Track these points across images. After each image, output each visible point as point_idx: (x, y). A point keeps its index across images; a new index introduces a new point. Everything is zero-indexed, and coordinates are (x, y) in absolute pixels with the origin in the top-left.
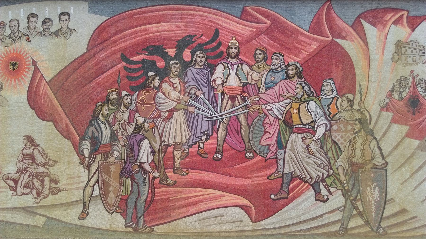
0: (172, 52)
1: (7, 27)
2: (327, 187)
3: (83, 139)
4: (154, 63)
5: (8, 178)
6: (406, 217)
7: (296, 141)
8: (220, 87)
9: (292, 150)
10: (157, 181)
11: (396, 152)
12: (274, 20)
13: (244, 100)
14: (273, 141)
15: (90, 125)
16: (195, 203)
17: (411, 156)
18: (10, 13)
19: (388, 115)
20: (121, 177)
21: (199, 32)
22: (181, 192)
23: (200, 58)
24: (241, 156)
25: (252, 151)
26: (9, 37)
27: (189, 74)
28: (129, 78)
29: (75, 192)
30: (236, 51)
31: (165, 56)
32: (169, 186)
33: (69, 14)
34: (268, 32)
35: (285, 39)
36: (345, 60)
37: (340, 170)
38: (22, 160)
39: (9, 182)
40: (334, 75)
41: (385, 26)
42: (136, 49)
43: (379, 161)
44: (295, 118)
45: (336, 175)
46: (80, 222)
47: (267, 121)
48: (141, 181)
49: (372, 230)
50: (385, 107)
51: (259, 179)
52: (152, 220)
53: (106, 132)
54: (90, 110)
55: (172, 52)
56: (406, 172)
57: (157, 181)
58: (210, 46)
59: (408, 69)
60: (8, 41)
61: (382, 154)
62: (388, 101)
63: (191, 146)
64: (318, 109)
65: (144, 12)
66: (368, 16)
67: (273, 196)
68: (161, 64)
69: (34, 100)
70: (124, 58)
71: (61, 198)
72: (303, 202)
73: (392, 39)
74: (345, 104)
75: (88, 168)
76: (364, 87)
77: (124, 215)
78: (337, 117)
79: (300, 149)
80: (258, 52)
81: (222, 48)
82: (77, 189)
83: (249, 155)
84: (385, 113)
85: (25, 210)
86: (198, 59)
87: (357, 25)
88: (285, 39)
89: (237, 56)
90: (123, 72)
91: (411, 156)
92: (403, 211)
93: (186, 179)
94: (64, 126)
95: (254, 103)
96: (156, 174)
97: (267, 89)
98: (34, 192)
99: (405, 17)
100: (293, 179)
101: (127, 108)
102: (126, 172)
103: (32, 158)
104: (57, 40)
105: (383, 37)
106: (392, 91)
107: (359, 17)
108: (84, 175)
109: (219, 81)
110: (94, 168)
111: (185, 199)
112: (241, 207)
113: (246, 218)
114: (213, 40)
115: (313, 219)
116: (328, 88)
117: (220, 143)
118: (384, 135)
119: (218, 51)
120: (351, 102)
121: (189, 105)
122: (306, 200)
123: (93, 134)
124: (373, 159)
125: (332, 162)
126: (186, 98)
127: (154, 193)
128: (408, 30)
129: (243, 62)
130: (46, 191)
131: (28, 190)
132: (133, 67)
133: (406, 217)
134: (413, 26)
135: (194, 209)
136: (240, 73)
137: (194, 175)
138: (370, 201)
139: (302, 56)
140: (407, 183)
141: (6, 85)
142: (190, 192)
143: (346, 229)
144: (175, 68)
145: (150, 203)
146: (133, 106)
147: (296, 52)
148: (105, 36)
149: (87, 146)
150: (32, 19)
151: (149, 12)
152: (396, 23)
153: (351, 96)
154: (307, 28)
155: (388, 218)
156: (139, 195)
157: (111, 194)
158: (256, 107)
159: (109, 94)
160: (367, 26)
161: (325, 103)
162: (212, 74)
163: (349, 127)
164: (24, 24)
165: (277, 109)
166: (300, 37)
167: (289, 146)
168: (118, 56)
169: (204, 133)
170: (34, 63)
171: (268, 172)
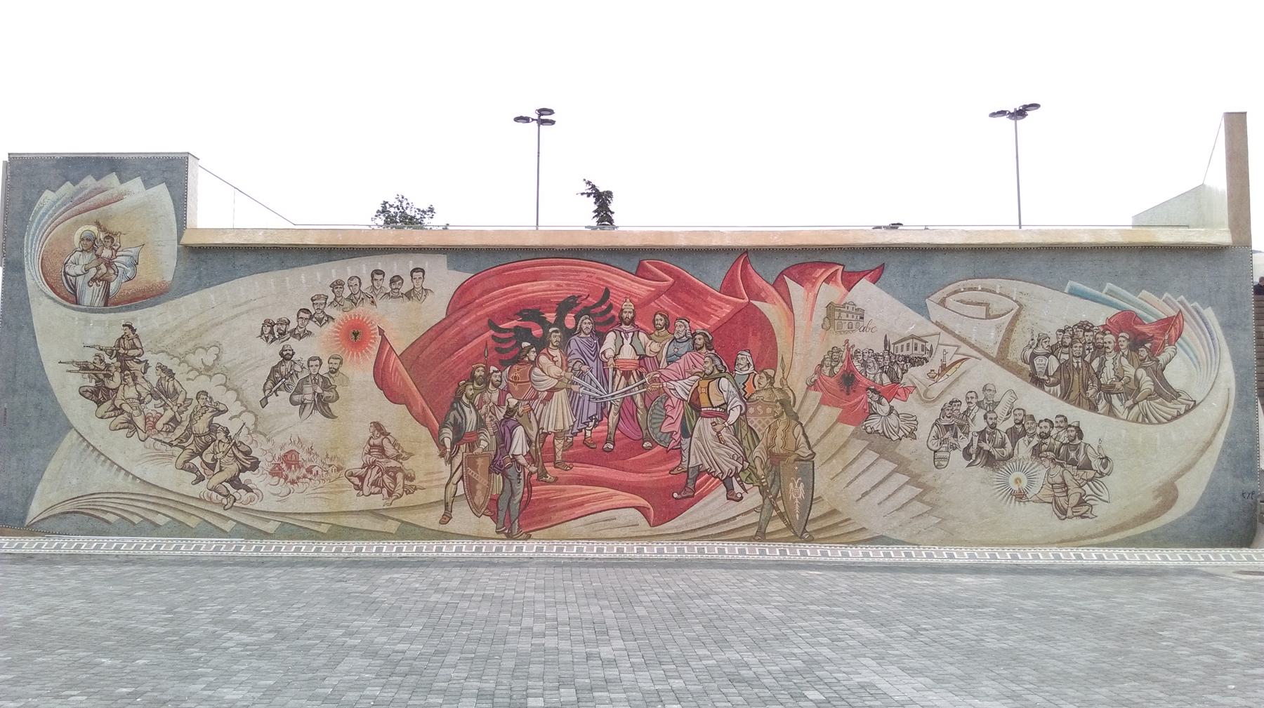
0: (551, 317)
1: (346, 286)
2: (741, 483)
3: (443, 426)
4: (530, 330)
5: (352, 475)
6: (837, 519)
7: (704, 427)
8: (611, 361)
9: (699, 438)
10: (535, 477)
11: (825, 441)
12: (677, 277)
13: (641, 377)
14: (677, 427)
15: (452, 408)
16: (582, 504)
17: (844, 446)
18: (349, 269)
19: (816, 395)
20: (490, 472)
21: (584, 292)
22: (564, 490)
23: (586, 324)
24: (637, 446)
25: (651, 440)
26: (349, 299)
27: (573, 344)
28: (498, 350)
29: (435, 491)
30: (631, 315)
31: (543, 322)
32: (549, 483)
33: (423, 271)
34: (670, 291)
35: (691, 301)
36: (764, 327)
37: (757, 462)
38: (369, 453)
39: (353, 479)
40: (750, 347)
41: (814, 284)
42: (506, 314)
44: (703, 398)
45: (752, 468)
46: (442, 528)
47: (669, 402)
48: (514, 477)
49: (796, 535)
50: (813, 385)
51: (659, 475)
52: (529, 525)
53: (471, 417)
54: (451, 390)
55: (551, 317)
56: (837, 464)
57: (535, 477)
58: (598, 310)
59: (843, 337)
60: (347, 304)
61: (808, 442)
62: (816, 377)
63: (575, 434)
64: (731, 388)
65: (517, 268)
66: (794, 272)
67: (675, 495)
68: (537, 332)
69: (382, 377)
70: (492, 325)
71: (418, 498)
72: (712, 501)
73: (822, 301)
74: (764, 382)
75: (450, 461)
76: (787, 361)
77: (495, 518)
78: (754, 397)
79: (710, 437)
80: (658, 317)
81: (613, 312)
82: (437, 486)
83: (646, 444)
84: (812, 393)
85: (374, 513)
86: (584, 326)
87: (779, 284)
88: (691, 301)
89: (632, 322)
90: (491, 343)
91: (844, 446)
92: (834, 512)
93: (569, 474)
94: (420, 410)
95: (653, 380)
96: (533, 469)
97: (669, 362)
98: (385, 491)
99: (840, 273)
100: (700, 473)
101: (497, 387)
102: (496, 467)
103: (382, 450)
104: (409, 303)
105: (811, 298)
106: (821, 366)
107: (782, 273)
108: (446, 470)
109: (610, 353)
110: (457, 461)
111: (569, 499)
112: (637, 508)
113: (643, 521)
114: (603, 301)
115: (724, 522)
116: (743, 362)
117: (612, 430)
118: (811, 419)
119: (609, 316)
120: (771, 380)
121: (573, 383)
122: (715, 499)
123: (455, 419)
124: (797, 449)
125: (748, 453)
126: (569, 375)
127: (530, 491)
128: (843, 289)
129: (639, 330)
130: (399, 490)
131: (377, 489)
132: (502, 336)
133: (837, 519)
135: (579, 511)
136: (636, 343)
137: (579, 470)
138: (793, 500)
139: (712, 322)
140: (838, 478)
141: (347, 359)
142: (575, 490)
143: (764, 533)
144: (555, 338)
145: (526, 503)
146: (504, 384)
147: (705, 317)
148: (468, 298)
149: (448, 435)
150: (376, 277)
151: (522, 267)
152: (827, 280)
153: (771, 372)
154: (718, 287)
155: (814, 520)
156: (513, 494)
157: (479, 493)
158: (656, 385)
159: (474, 370)
160: (791, 284)
161: (740, 381)
162: (601, 345)
163: (769, 410)
164: (366, 283)
165: (682, 388)
166: (709, 298)
167: (696, 434)
168: (485, 322)
169: (591, 418)
170: (381, 332)
171: (670, 466)
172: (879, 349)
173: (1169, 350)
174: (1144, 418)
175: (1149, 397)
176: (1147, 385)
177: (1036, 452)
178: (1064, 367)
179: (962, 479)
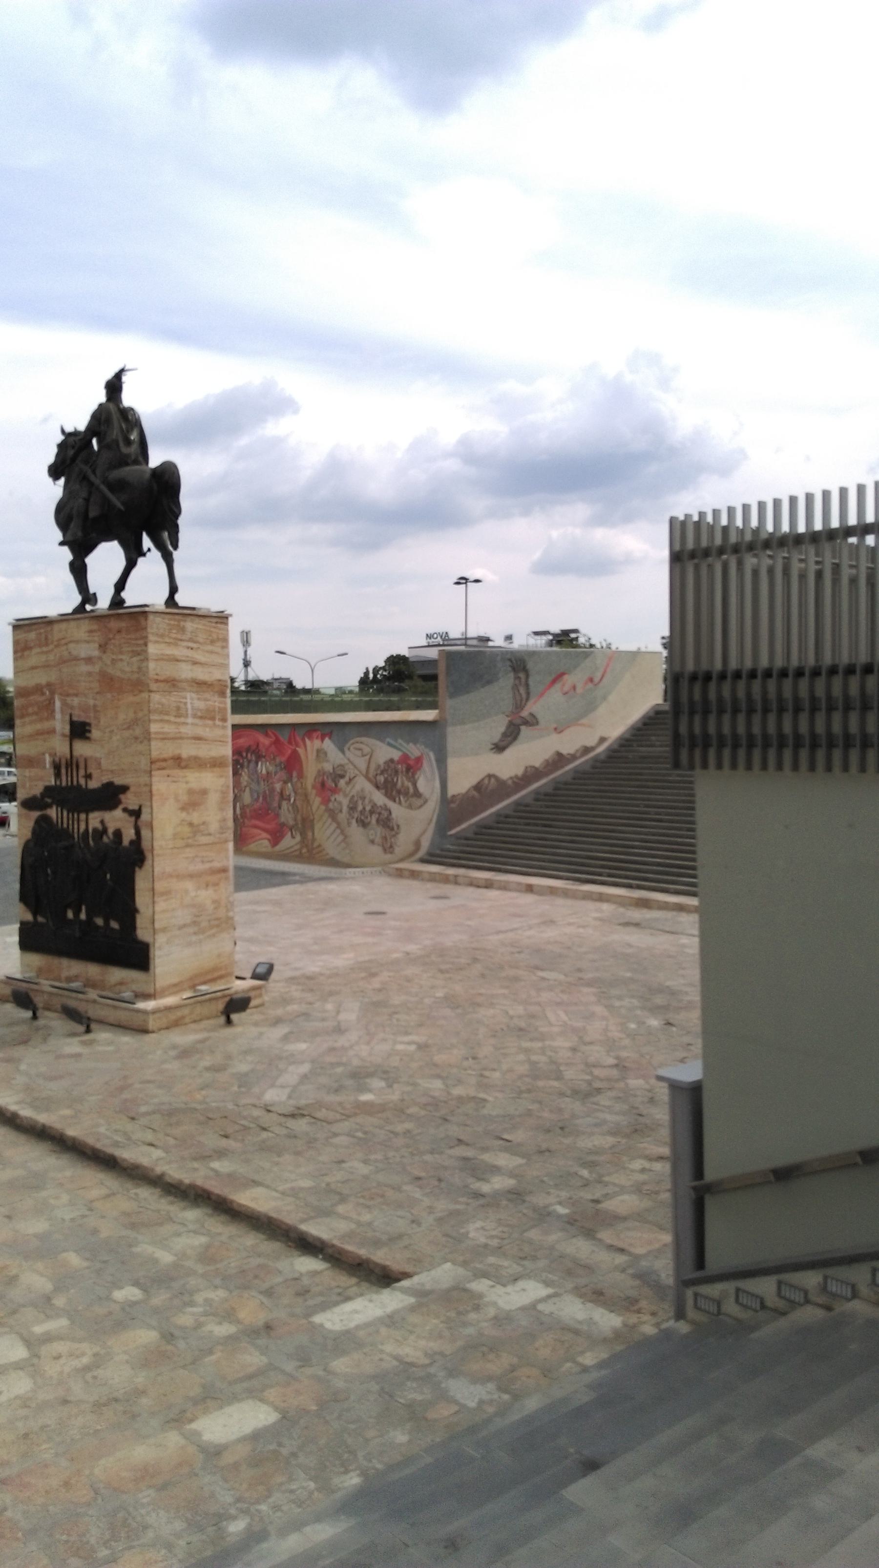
43: (312, 818)
134: (322, 740)
160: (307, 740)
165: (278, 786)
172: (331, 771)
173: (418, 773)
174: (410, 807)
175: (412, 796)
176: (411, 790)
177: (378, 821)
178: (386, 780)
179: (356, 832)
